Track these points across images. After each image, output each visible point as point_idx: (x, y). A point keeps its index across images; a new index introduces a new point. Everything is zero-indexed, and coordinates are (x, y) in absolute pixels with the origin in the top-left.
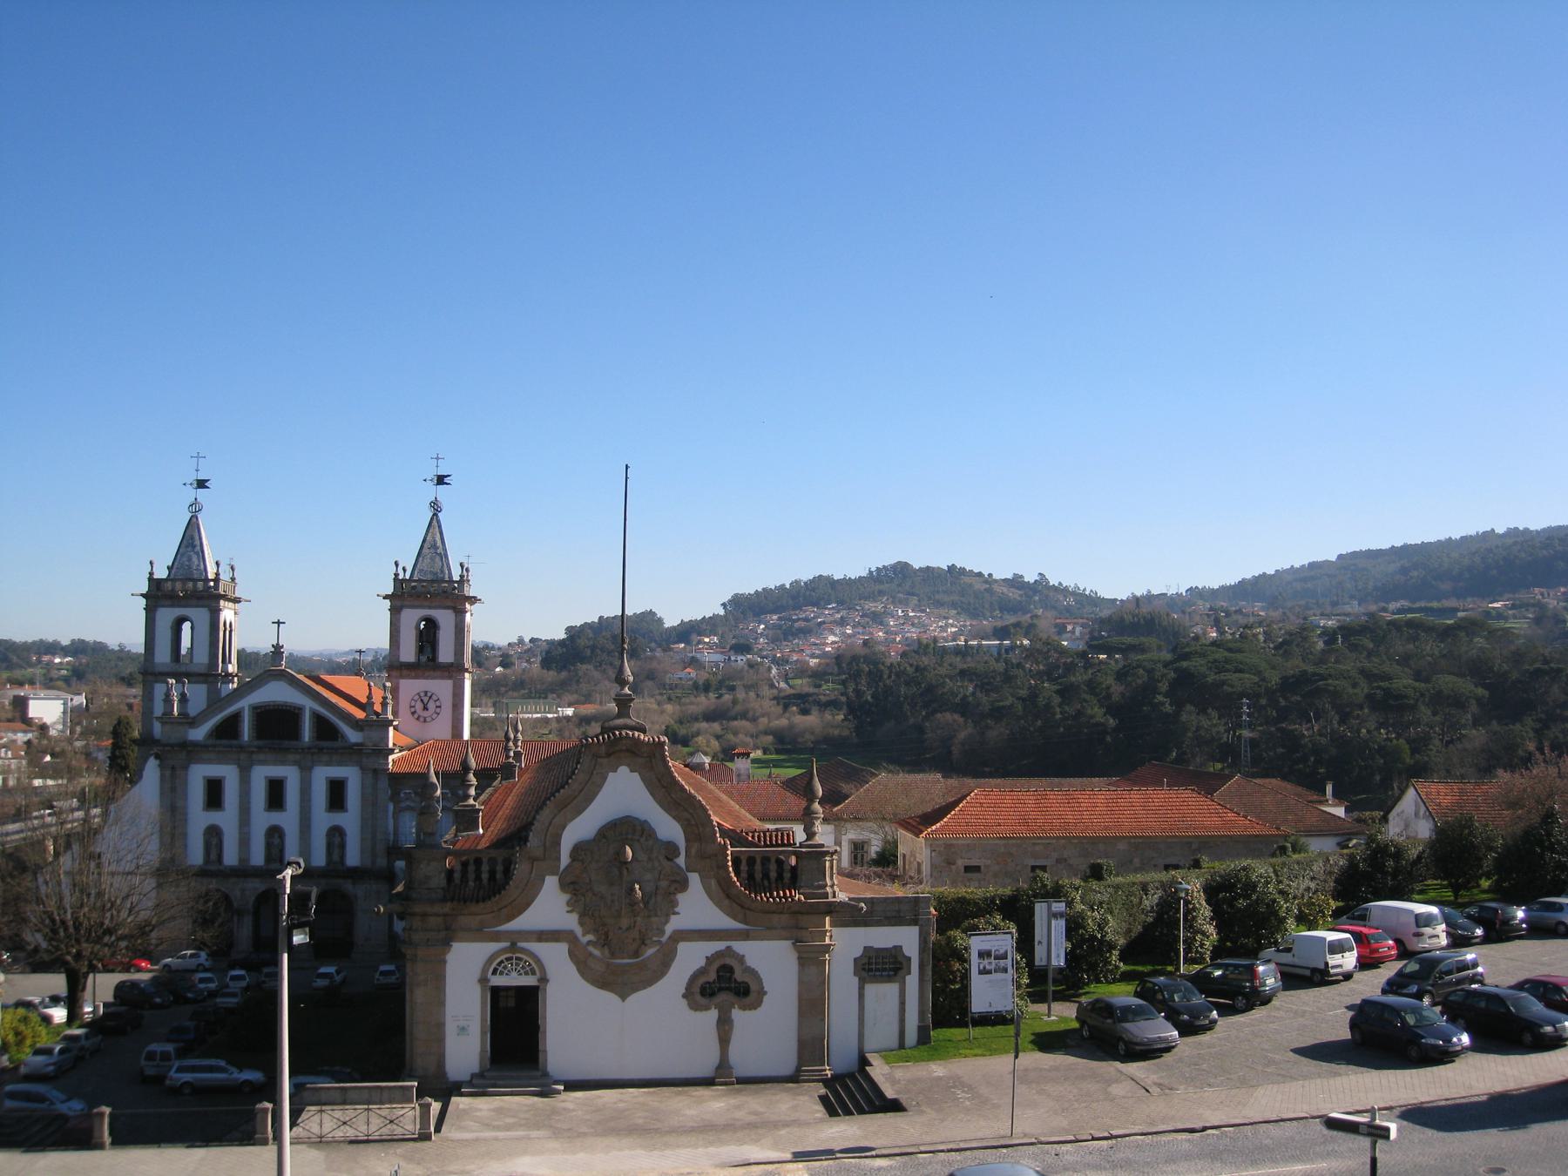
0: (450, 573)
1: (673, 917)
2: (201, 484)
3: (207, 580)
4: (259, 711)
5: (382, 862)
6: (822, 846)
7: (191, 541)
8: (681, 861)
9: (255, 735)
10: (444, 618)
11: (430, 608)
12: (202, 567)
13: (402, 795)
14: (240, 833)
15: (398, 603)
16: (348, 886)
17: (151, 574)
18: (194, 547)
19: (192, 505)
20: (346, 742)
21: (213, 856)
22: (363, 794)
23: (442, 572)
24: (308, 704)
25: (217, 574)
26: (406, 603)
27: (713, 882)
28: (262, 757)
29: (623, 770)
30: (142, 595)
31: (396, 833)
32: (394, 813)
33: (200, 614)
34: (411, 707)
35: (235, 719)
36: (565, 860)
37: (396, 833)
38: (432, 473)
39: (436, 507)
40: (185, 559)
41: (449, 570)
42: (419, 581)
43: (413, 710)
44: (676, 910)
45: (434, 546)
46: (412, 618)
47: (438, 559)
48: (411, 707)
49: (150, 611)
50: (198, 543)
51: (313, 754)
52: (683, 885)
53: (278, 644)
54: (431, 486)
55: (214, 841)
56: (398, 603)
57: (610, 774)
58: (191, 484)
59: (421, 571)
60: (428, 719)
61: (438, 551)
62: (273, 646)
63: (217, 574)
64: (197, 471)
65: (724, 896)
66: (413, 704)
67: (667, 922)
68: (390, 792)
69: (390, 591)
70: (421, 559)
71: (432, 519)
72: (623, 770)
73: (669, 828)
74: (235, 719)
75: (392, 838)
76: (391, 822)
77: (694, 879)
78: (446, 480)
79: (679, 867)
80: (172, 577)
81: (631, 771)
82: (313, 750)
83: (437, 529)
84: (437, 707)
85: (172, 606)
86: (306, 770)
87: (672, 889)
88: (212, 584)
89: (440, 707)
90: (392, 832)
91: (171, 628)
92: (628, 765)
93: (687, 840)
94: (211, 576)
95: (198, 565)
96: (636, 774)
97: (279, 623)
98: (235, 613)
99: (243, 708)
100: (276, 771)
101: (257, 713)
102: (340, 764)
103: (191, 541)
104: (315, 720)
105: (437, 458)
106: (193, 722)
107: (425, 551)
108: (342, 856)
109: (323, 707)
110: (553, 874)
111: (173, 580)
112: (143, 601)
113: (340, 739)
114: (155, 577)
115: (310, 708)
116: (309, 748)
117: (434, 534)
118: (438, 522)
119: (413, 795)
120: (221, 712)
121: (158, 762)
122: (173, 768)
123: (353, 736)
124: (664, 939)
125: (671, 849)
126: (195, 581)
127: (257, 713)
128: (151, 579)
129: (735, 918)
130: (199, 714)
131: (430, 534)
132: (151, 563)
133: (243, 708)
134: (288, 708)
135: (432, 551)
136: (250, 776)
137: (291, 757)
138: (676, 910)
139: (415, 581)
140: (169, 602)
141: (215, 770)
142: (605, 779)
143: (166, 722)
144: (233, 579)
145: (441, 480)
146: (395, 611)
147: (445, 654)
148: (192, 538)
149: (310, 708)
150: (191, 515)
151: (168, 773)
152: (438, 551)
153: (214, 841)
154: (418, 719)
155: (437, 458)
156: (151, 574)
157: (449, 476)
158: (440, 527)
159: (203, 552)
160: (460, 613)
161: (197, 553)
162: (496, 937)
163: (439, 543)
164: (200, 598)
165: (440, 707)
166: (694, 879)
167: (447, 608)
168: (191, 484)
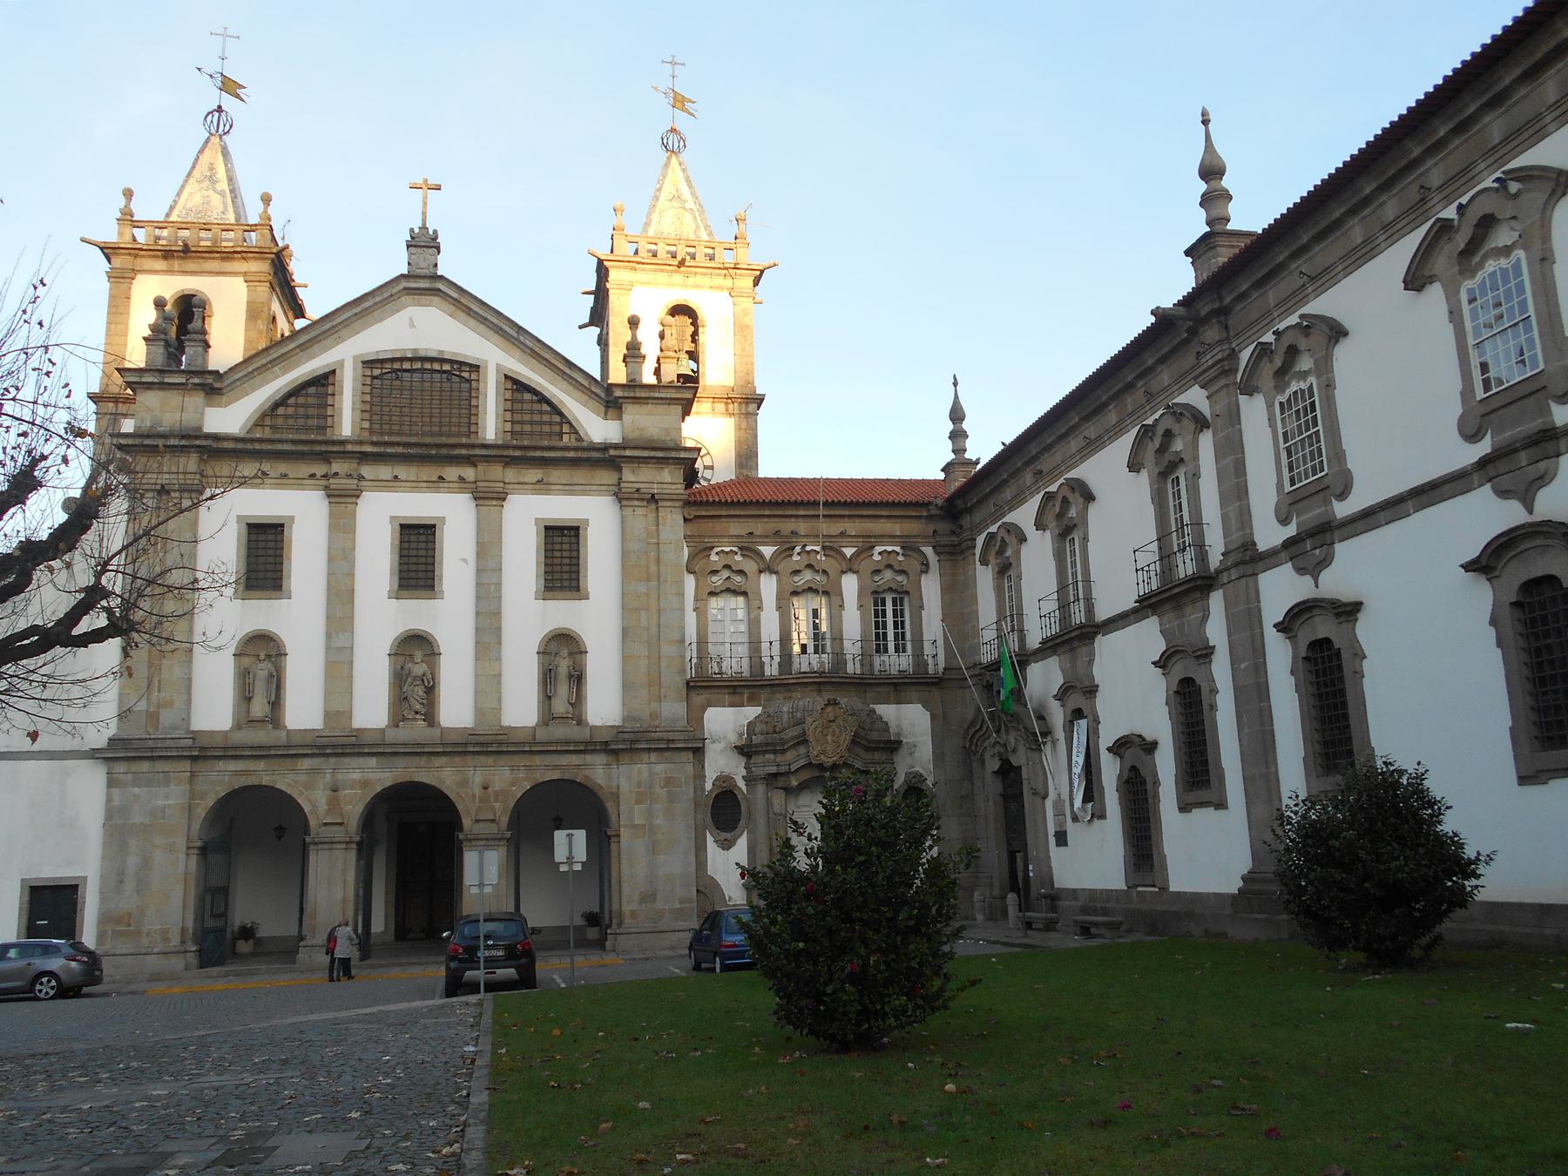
4: (377, 372)
5: (673, 710)
9: (366, 425)
13: (714, 558)
14: (328, 648)
16: (598, 771)
20: (580, 439)
21: (259, 708)
22: (625, 554)
24: (495, 358)
28: (385, 472)
31: (702, 642)
32: (696, 599)
35: (324, 381)
37: (702, 642)
38: (666, 84)
49: (121, 279)
53: (424, 228)
54: (664, 104)
55: (262, 670)
62: (412, 230)
68: (686, 550)
74: (324, 381)
75: (692, 653)
76: (691, 619)
86: (488, 497)
90: (694, 640)
99: (341, 363)
100: (419, 505)
102: (570, 489)
106: (213, 386)
107: (663, 202)
108: (578, 701)
115: (498, 366)
119: (738, 558)
120: (286, 371)
123: (598, 428)
133: (341, 363)
134: (447, 367)
135: (676, 204)
136: (353, 515)
137: (452, 473)
140: (161, 265)
141: (264, 502)
149: (498, 366)
152: (688, 206)
153: (262, 670)
161: (222, 194)
167: (720, 288)
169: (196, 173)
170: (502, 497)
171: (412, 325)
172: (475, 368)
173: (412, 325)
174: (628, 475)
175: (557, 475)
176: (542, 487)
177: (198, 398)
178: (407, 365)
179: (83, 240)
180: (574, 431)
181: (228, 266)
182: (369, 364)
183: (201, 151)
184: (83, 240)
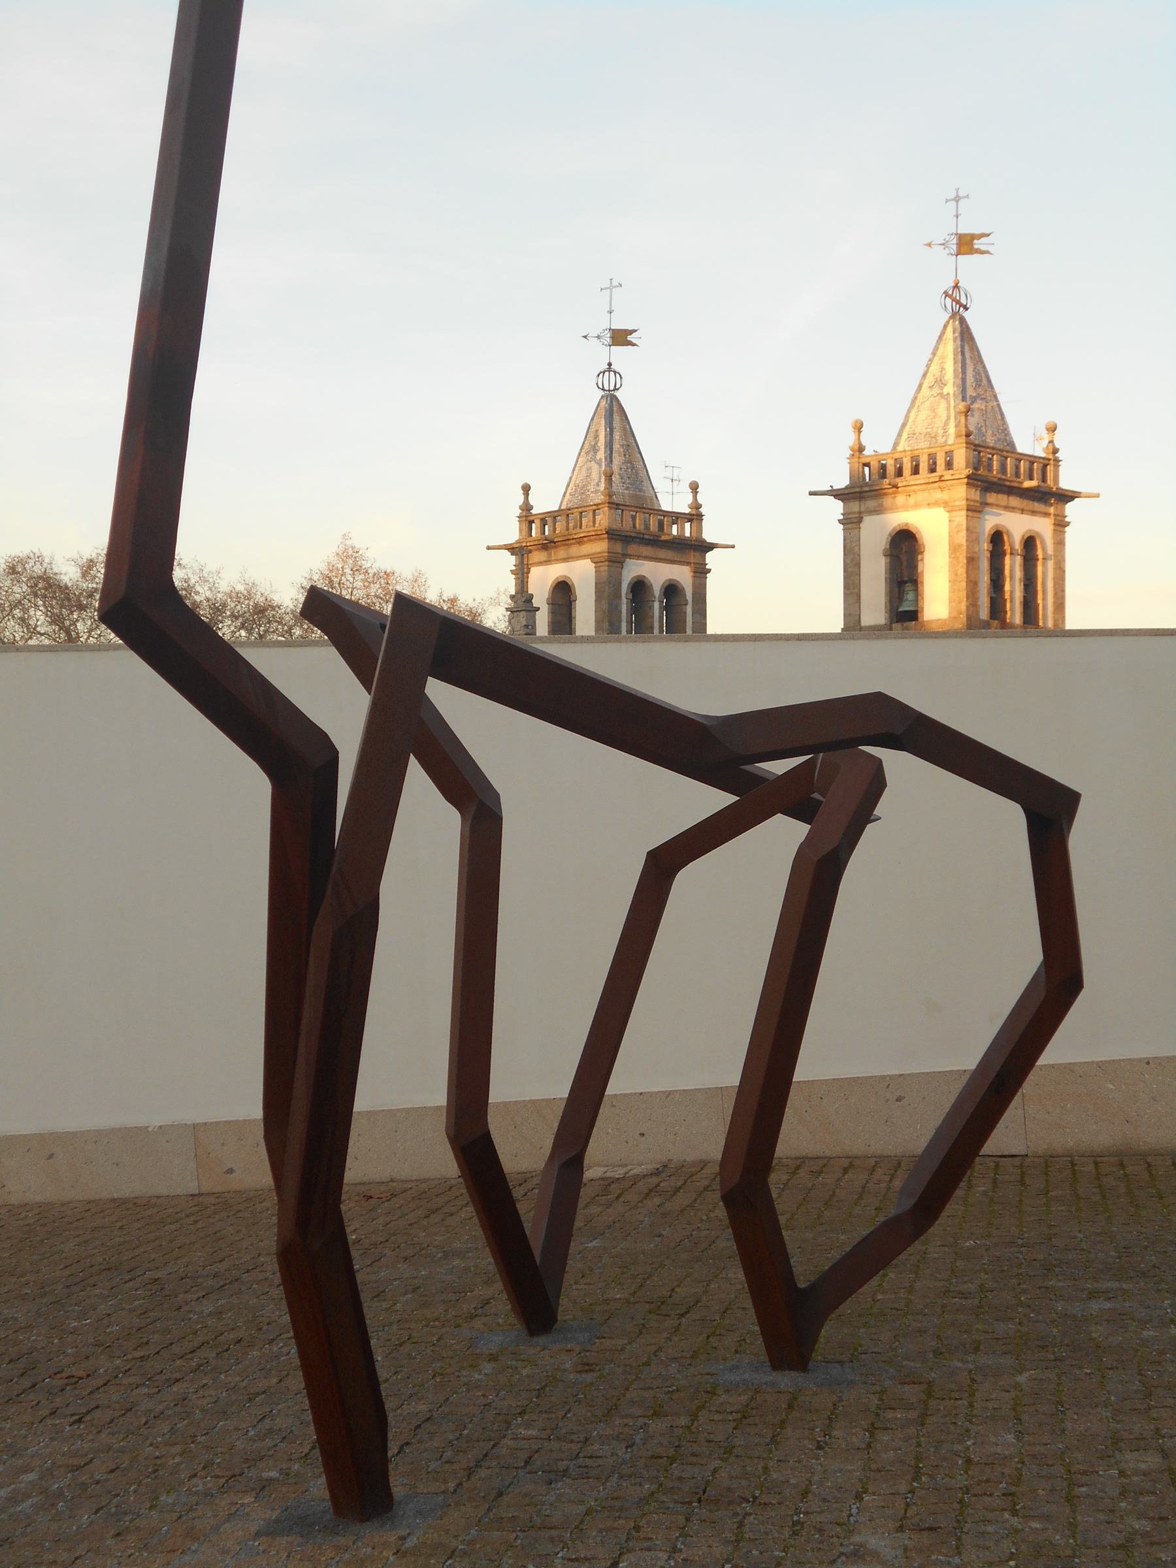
2: (620, 338)
17: (527, 507)
38: (945, 229)
56: (855, 506)
58: (598, 337)
61: (945, 391)
69: (842, 481)
70: (914, 411)
78: (978, 244)
112: (511, 561)
117: (943, 358)
135: (935, 391)
145: (966, 244)
146: (851, 523)
155: (957, 199)
156: (527, 507)
157: (988, 235)
168: (598, 337)
179: (489, 548)
183: (592, 419)
184: (489, 548)
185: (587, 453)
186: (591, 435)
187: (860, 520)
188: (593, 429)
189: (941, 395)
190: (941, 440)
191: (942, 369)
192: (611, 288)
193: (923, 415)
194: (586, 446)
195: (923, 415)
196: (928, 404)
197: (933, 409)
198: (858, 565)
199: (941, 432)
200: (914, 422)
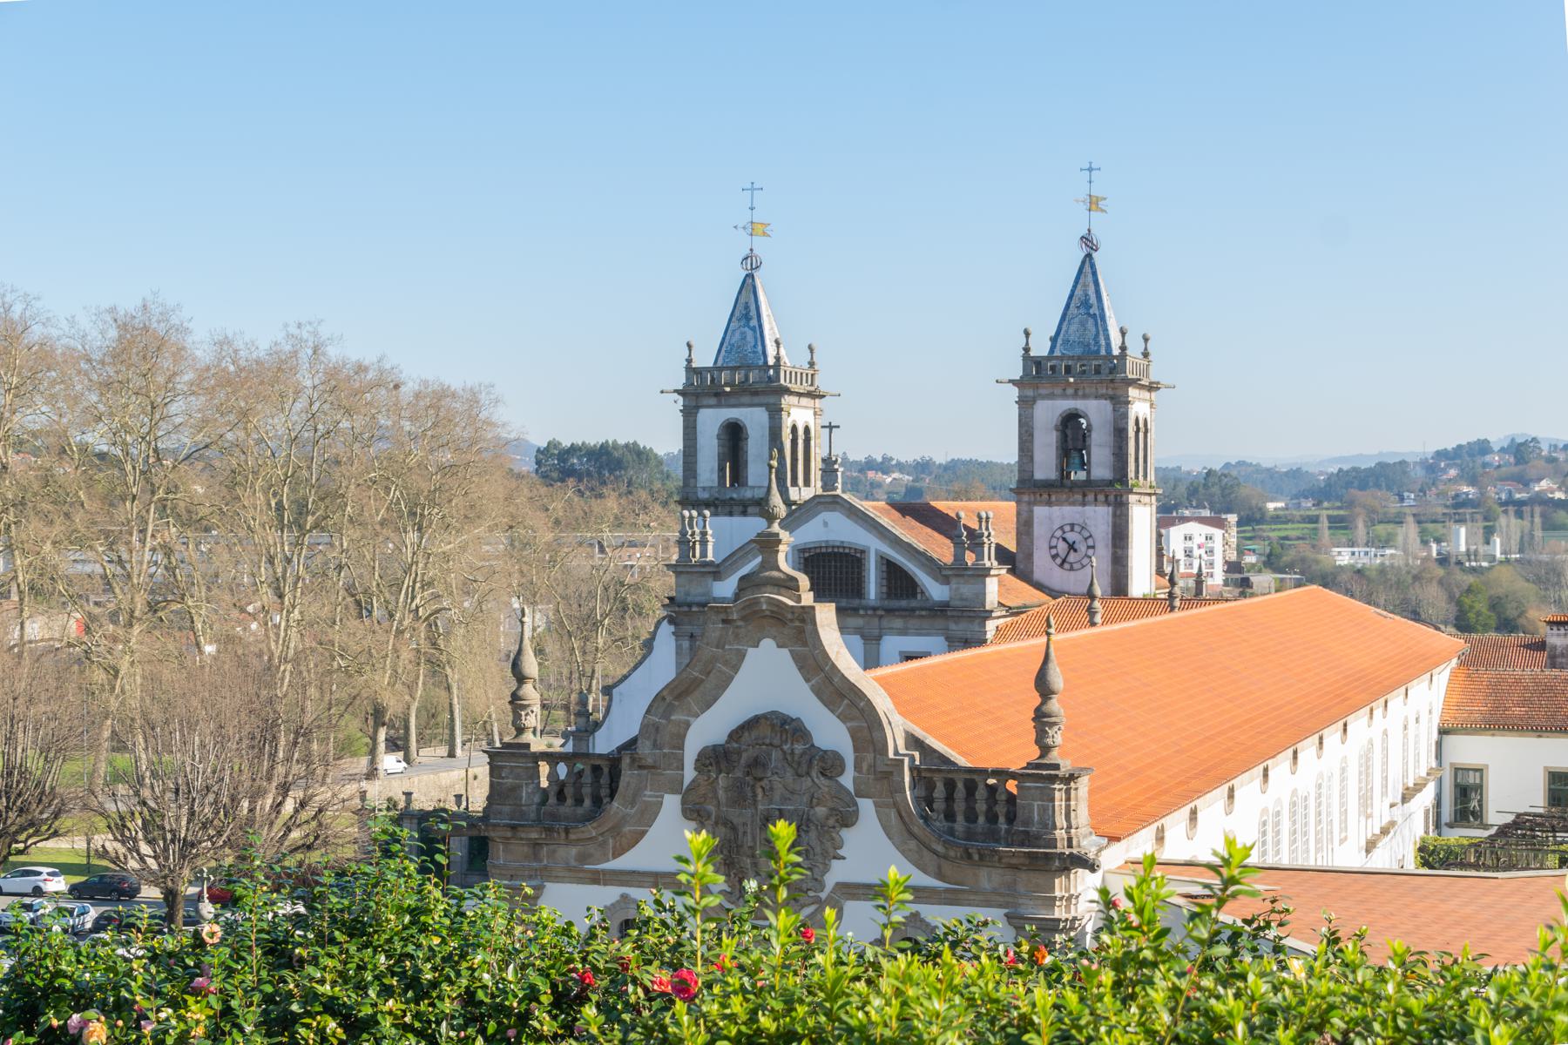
0: (1108, 345)
1: (835, 863)
3: (766, 366)
4: (807, 555)
6: (1057, 767)
7: (746, 312)
8: (847, 780)
10: (1095, 411)
11: (1075, 396)
12: (760, 348)
15: (1030, 393)
17: (689, 361)
18: (747, 317)
19: (746, 258)
23: (1097, 342)
24: (874, 546)
25: (778, 358)
26: (1043, 391)
27: (893, 814)
29: (768, 644)
30: (676, 391)
33: (753, 419)
34: (1051, 548)
36: (689, 774)
39: (1088, 241)
40: (737, 336)
41: (1107, 338)
42: (1061, 358)
43: (1054, 552)
44: (841, 852)
45: (1086, 304)
46: (1048, 412)
47: (1091, 321)
48: (1051, 548)
49: (690, 414)
50: (753, 313)
51: (881, 617)
52: (847, 818)
56: (1030, 393)
57: (751, 650)
58: (744, 228)
59: (1066, 342)
60: (1075, 566)
61: (1091, 311)
63: (778, 358)
64: (752, 209)
65: (905, 834)
66: (1053, 544)
67: (826, 868)
70: (1065, 323)
71: (1083, 263)
72: (768, 644)
73: (830, 733)
77: (866, 806)
79: (841, 786)
80: (719, 364)
81: (779, 646)
82: (880, 612)
83: (1090, 278)
84: (1089, 547)
85: (719, 405)
87: (831, 822)
88: (771, 372)
89: (1093, 547)
91: (719, 437)
92: (774, 638)
93: (856, 749)
94: (771, 361)
95: (755, 346)
96: (785, 652)
97: (831, 427)
98: (815, 414)
101: (806, 559)
102: (919, 633)
103: (746, 312)
104: (884, 568)
105: (1090, 170)
107: (1072, 309)
109: (893, 548)
110: (674, 791)
111: (721, 369)
113: (919, 596)
114: (694, 365)
116: (875, 609)
117: (1085, 285)
118: (1093, 266)
121: (672, 628)
122: (692, 636)
123: (937, 591)
124: (823, 895)
125: (830, 764)
126: (749, 367)
127: (806, 559)
128: (690, 370)
129: (925, 871)
130: (725, 560)
131: (1079, 286)
132: (689, 346)
135: (1082, 311)
138: (841, 852)
139: (1057, 358)
140: (713, 401)
142: (741, 656)
143: (681, 572)
144: (812, 364)
146: (1025, 404)
147: (1101, 466)
148: (747, 307)
150: (744, 273)
151: (686, 644)
152: (1091, 311)
154: (1061, 565)
155: (1090, 170)
156: (689, 361)
158: (1094, 274)
159: (761, 326)
160: (1120, 404)
161: (753, 329)
162: (598, 878)
163: (1093, 300)
164: (755, 393)
165: (1093, 547)
166: (866, 806)
168: (744, 228)
169: (737, 314)
170: (879, 638)
171: (826, 524)
172: (863, 552)
173: (826, 524)
174: (953, 626)
175: (913, 623)
176: (903, 632)
177: (710, 580)
178: (824, 550)
180: (922, 593)
181: (756, 400)
182: (803, 551)
183: (740, 292)
185: (739, 320)
186: (740, 307)
187: (1034, 401)
188: (742, 300)
189: (1089, 314)
190: (1093, 348)
191: (1086, 295)
192: (753, 189)
193: (1073, 328)
194: (737, 314)
195: (1073, 328)
196: (1077, 320)
197: (1083, 324)
198: (1032, 435)
199: (1092, 342)
200: (1067, 332)
